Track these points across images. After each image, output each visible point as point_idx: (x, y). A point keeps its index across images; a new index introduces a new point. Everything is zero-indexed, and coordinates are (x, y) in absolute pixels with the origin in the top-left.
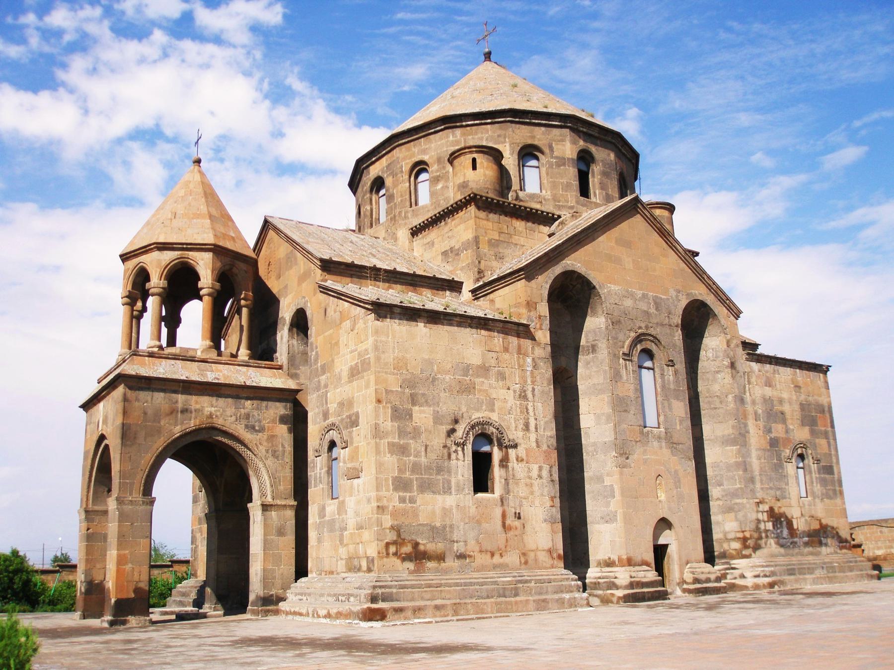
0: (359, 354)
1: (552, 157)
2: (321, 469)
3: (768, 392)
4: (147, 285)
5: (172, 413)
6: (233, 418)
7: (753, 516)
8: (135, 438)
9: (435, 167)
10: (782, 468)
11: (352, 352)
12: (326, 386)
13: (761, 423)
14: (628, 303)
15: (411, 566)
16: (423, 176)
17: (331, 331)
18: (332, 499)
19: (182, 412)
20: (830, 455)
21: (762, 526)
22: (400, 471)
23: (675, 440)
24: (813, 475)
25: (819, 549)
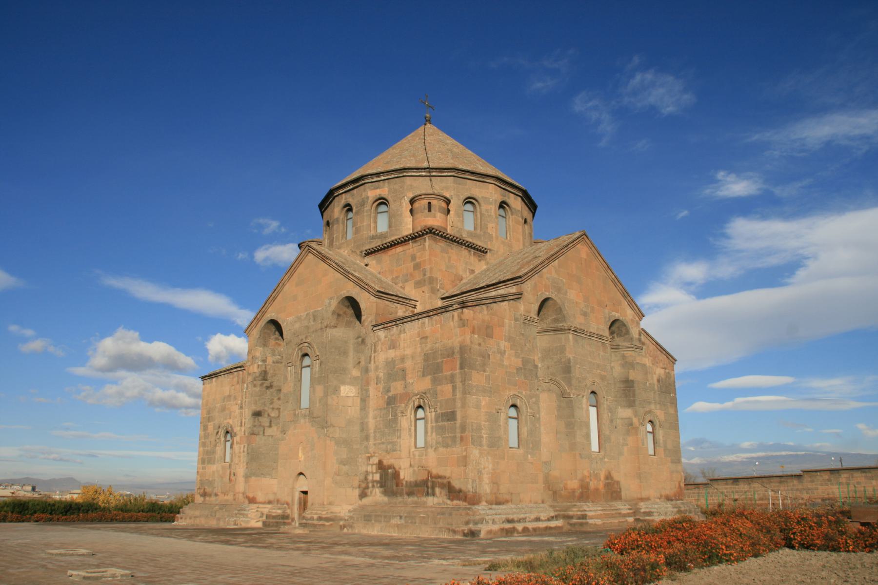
3: (392, 354)
7: (363, 469)
10: (397, 423)
13: (381, 386)
15: (202, 499)
20: (454, 400)
21: (370, 478)
23: (315, 415)
24: (429, 426)
25: (424, 499)
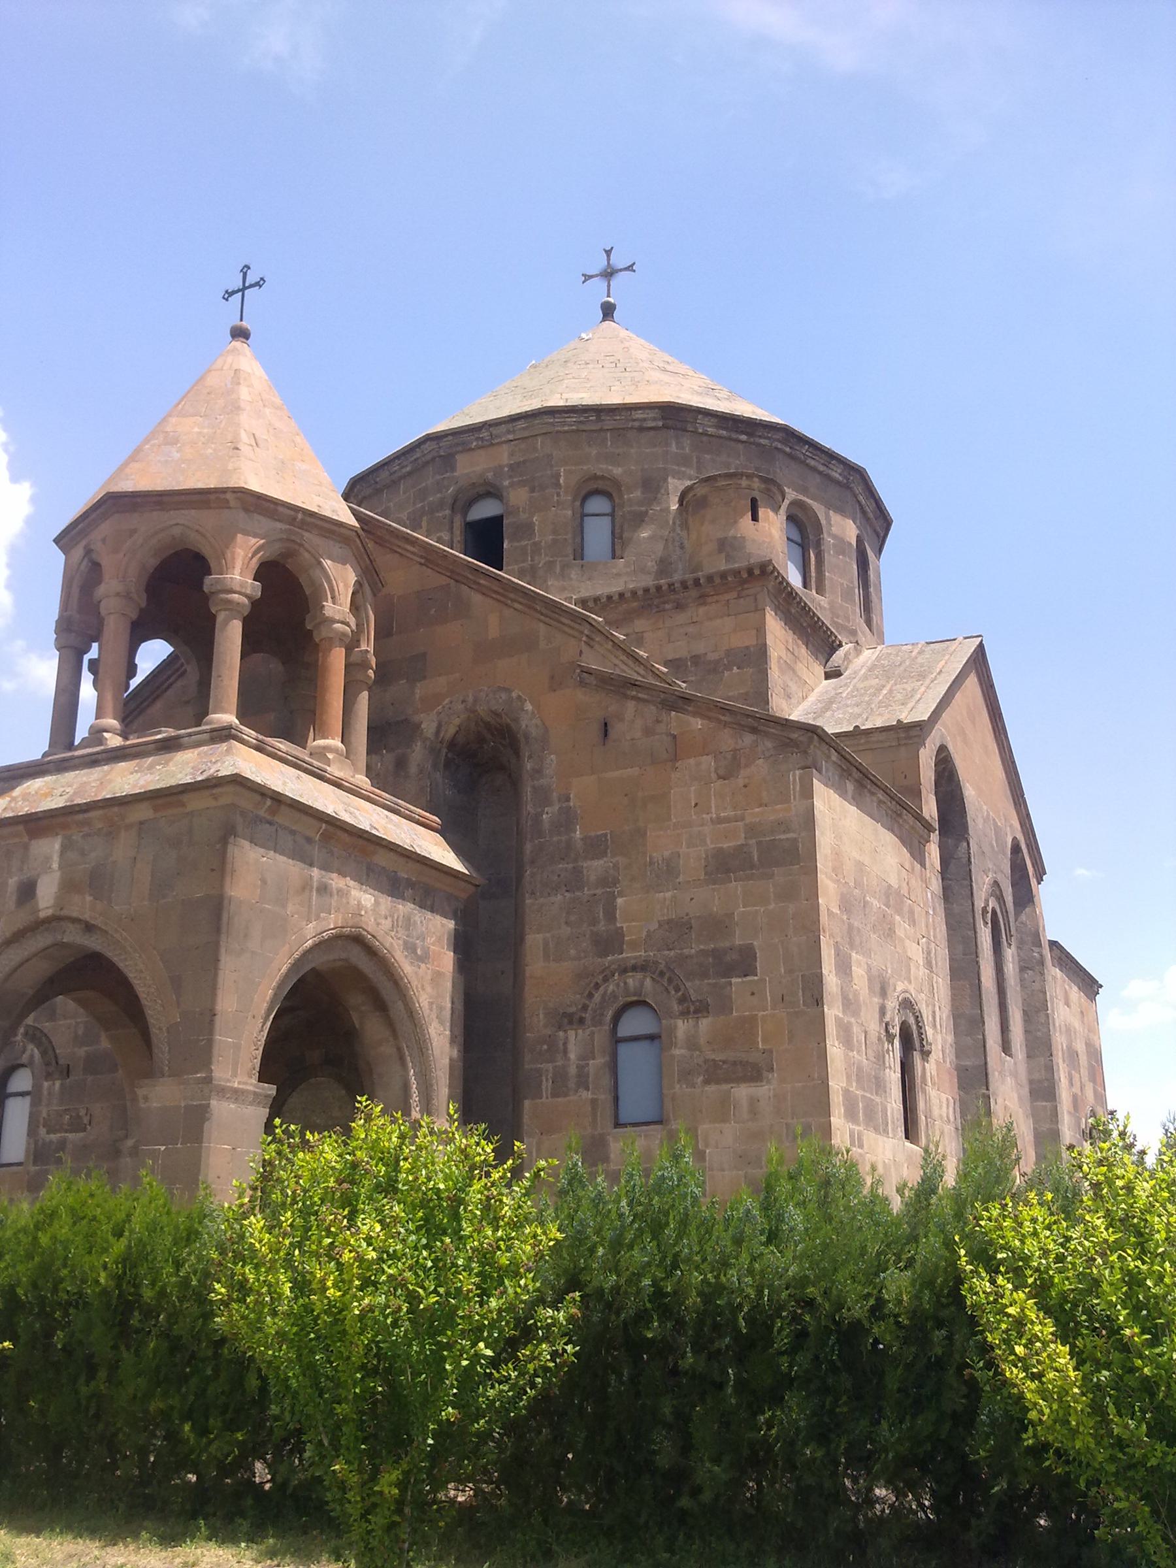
0: (751, 830)
1: (829, 534)
2: (583, 1057)
4: (208, 580)
5: (304, 889)
6: (386, 924)
8: (246, 936)
9: (637, 494)
11: (720, 820)
12: (608, 881)
14: (980, 822)
16: (598, 505)
17: (634, 771)
18: (617, 1125)
19: (319, 890)
22: (849, 1077)
